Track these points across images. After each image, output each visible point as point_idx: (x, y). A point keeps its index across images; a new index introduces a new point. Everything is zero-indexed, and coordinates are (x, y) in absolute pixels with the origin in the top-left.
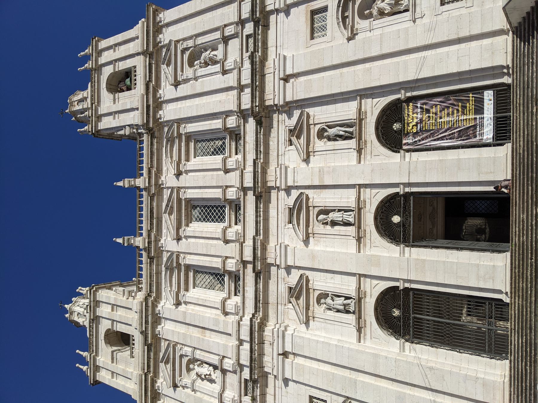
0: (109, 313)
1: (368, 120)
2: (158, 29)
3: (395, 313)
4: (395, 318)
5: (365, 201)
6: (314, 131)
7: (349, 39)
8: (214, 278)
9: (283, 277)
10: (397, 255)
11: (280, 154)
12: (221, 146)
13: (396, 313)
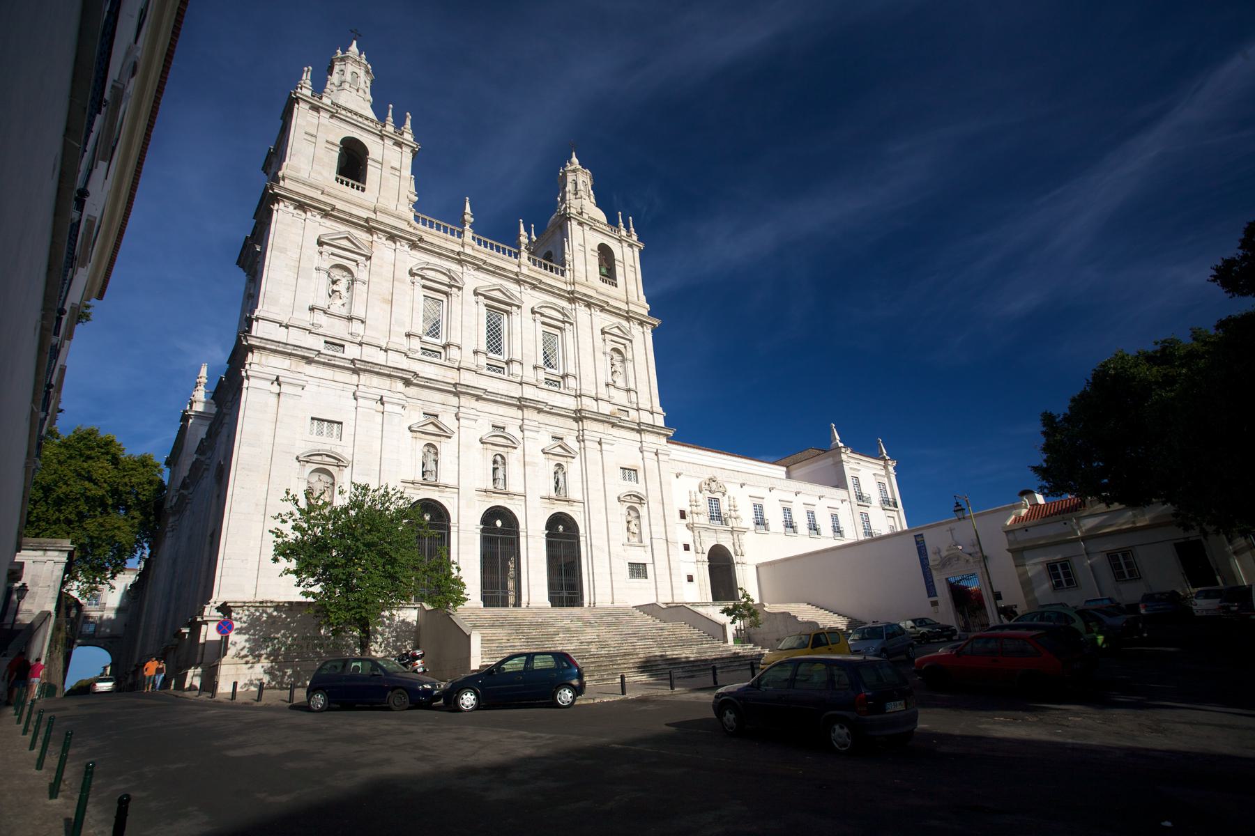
0: (390, 163)
1: (567, 507)
2: (641, 323)
3: (427, 516)
4: (423, 515)
5: (513, 499)
6: (562, 460)
7: (619, 498)
8: (434, 325)
9: (447, 411)
11: (547, 427)
12: (550, 364)
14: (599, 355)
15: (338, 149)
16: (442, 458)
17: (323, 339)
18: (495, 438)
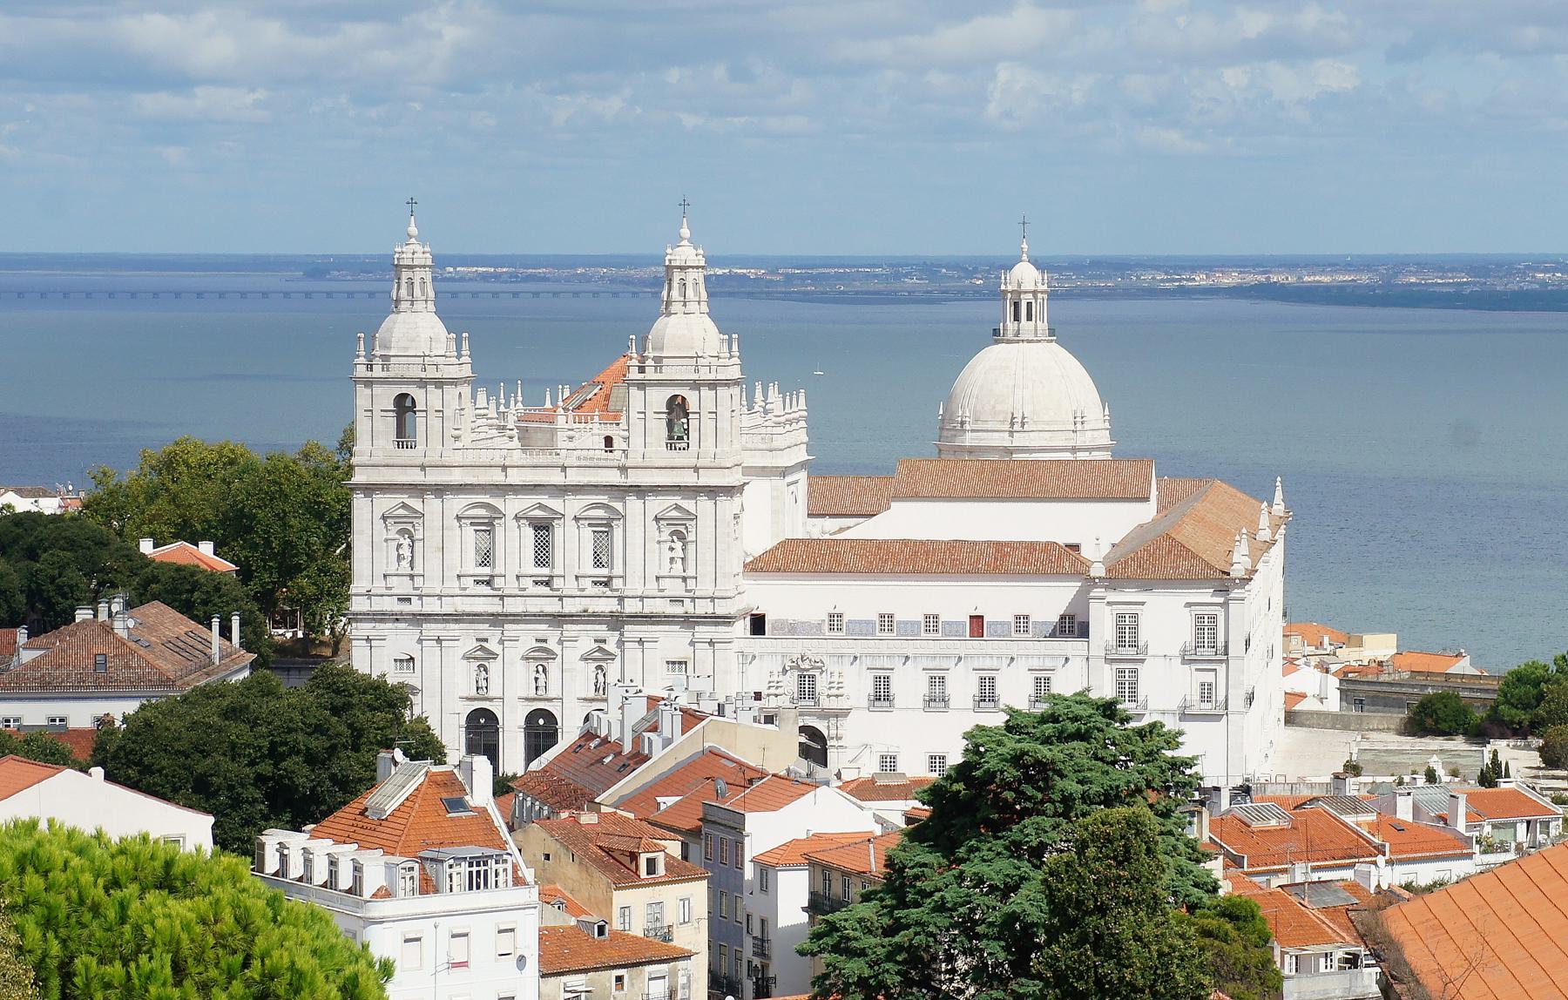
10: (519, 724)
13: (482, 721)
14: (652, 546)
16: (491, 675)
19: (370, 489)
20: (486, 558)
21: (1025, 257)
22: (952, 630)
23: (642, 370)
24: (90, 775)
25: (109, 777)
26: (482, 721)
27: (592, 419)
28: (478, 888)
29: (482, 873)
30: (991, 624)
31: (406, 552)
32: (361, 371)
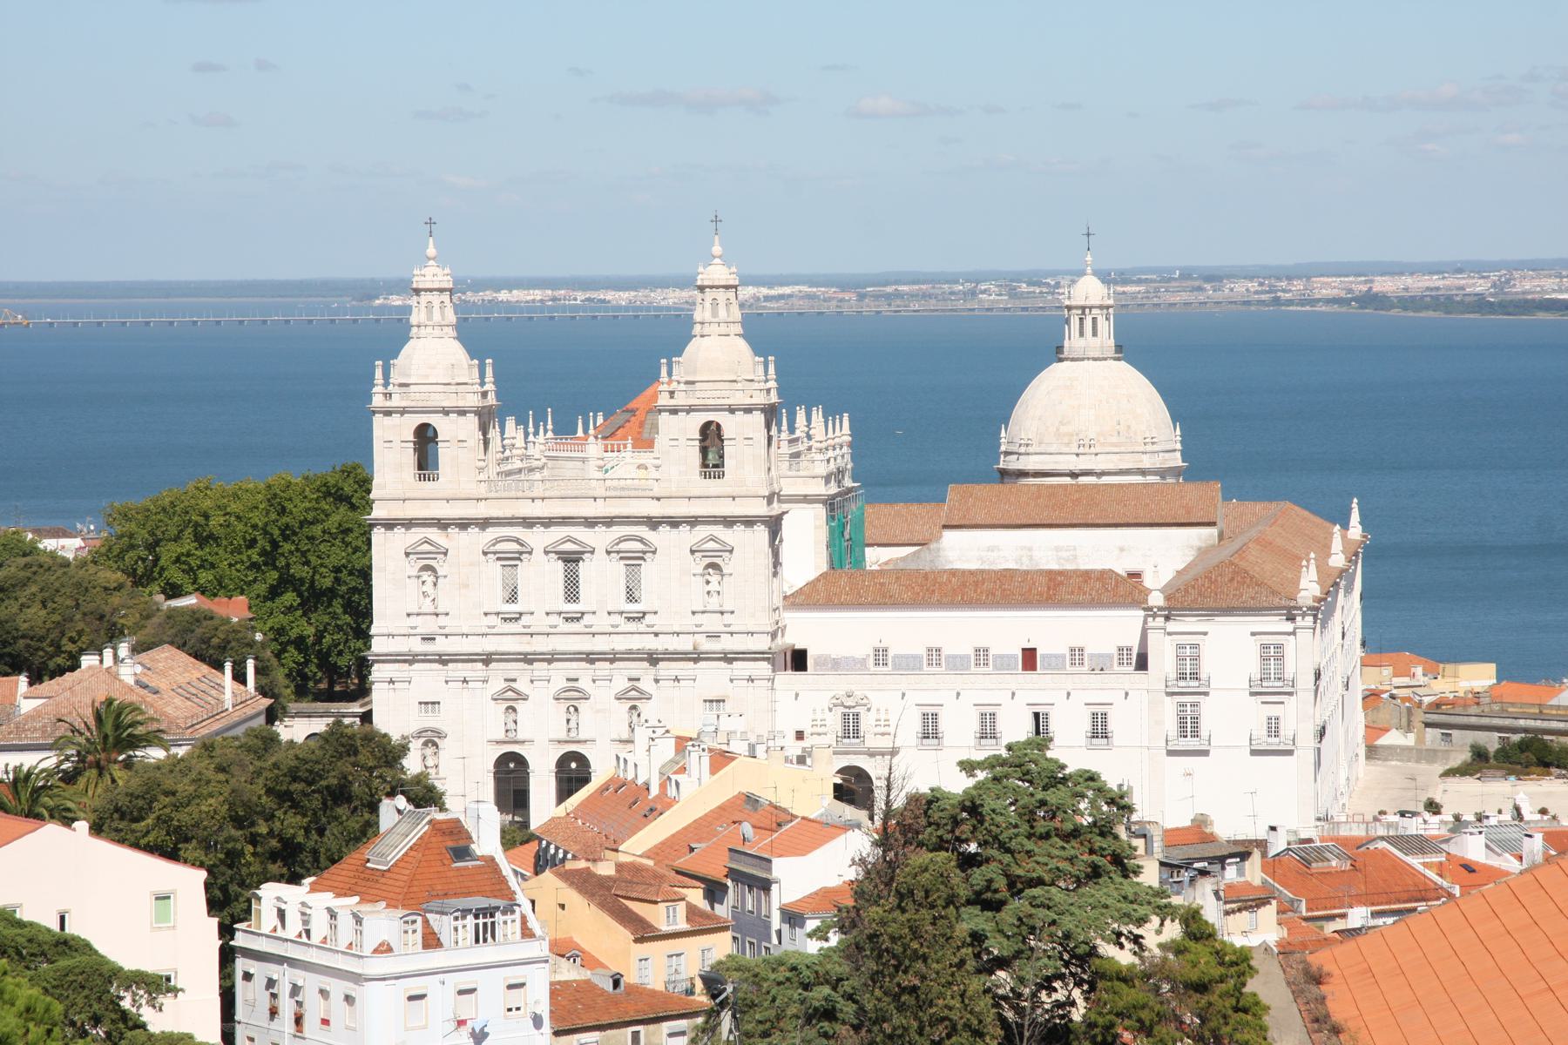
13: (512, 765)
15: (412, 445)
17: (419, 638)
18: (567, 694)
19: (390, 525)
20: (513, 597)
21: (1089, 270)
22: (1003, 663)
23: (388, 396)
24: (74, 830)
25: (97, 829)
26: (512, 765)
27: (625, 447)
28: (485, 940)
29: (489, 925)
30: (1043, 656)
31: (428, 588)
32: (378, 401)
